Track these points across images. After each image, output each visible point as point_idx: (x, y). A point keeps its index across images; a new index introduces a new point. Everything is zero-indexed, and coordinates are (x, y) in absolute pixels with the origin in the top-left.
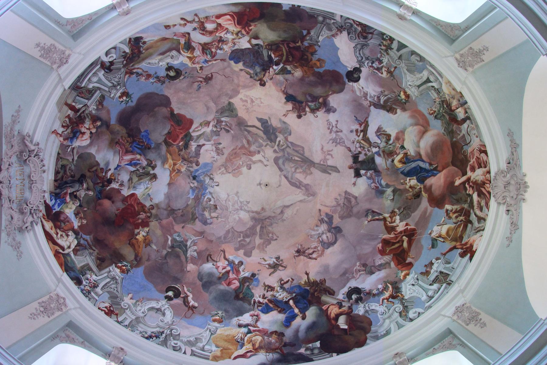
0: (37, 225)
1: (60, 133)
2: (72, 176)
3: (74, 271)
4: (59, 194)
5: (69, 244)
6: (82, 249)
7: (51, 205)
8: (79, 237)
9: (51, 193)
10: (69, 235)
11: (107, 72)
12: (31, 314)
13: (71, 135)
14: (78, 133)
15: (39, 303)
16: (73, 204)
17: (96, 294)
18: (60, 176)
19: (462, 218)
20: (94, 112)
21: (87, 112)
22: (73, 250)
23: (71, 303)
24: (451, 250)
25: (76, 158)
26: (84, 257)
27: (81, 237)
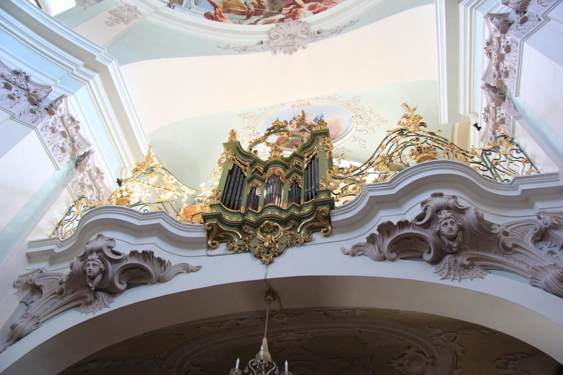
19: (252, 8)
24: (213, 4)
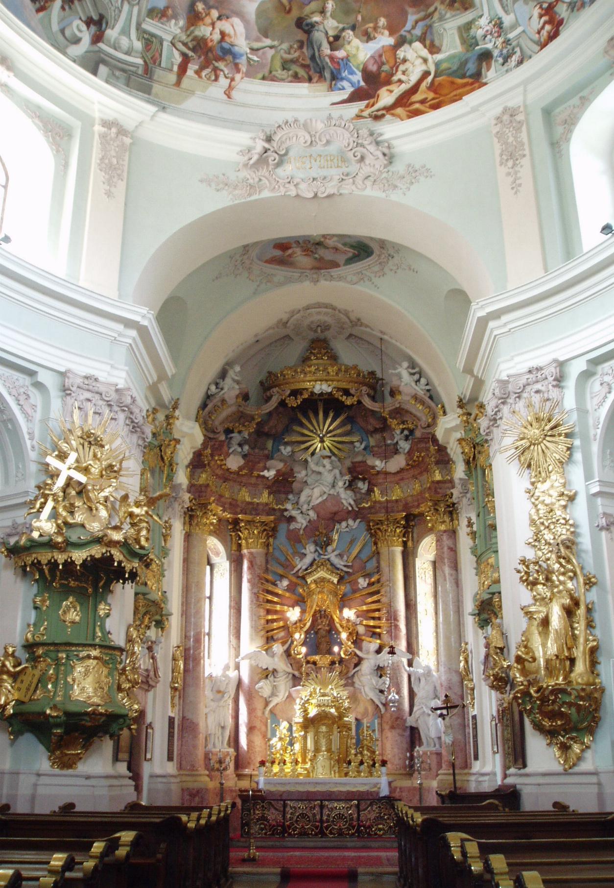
0: (381, 135)
1: (229, 81)
2: (301, 47)
3: (466, 61)
4: (332, 73)
5: (420, 61)
6: (432, 34)
7: (352, 89)
8: (408, 36)
9: (331, 88)
10: (405, 57)
11: (107, 23)
12: (513, 188)
13: (229, 58)
14: (225, 45)
15: (501, 164)
16: (349, 43)
17: (513, 27)
18: (302, 72)
20: (181, 23)
21: (184, 38)
22: (432, 53)
23: (515, 100)
25: (268, 42)
26: (445, 33)
27: (409, 32)
